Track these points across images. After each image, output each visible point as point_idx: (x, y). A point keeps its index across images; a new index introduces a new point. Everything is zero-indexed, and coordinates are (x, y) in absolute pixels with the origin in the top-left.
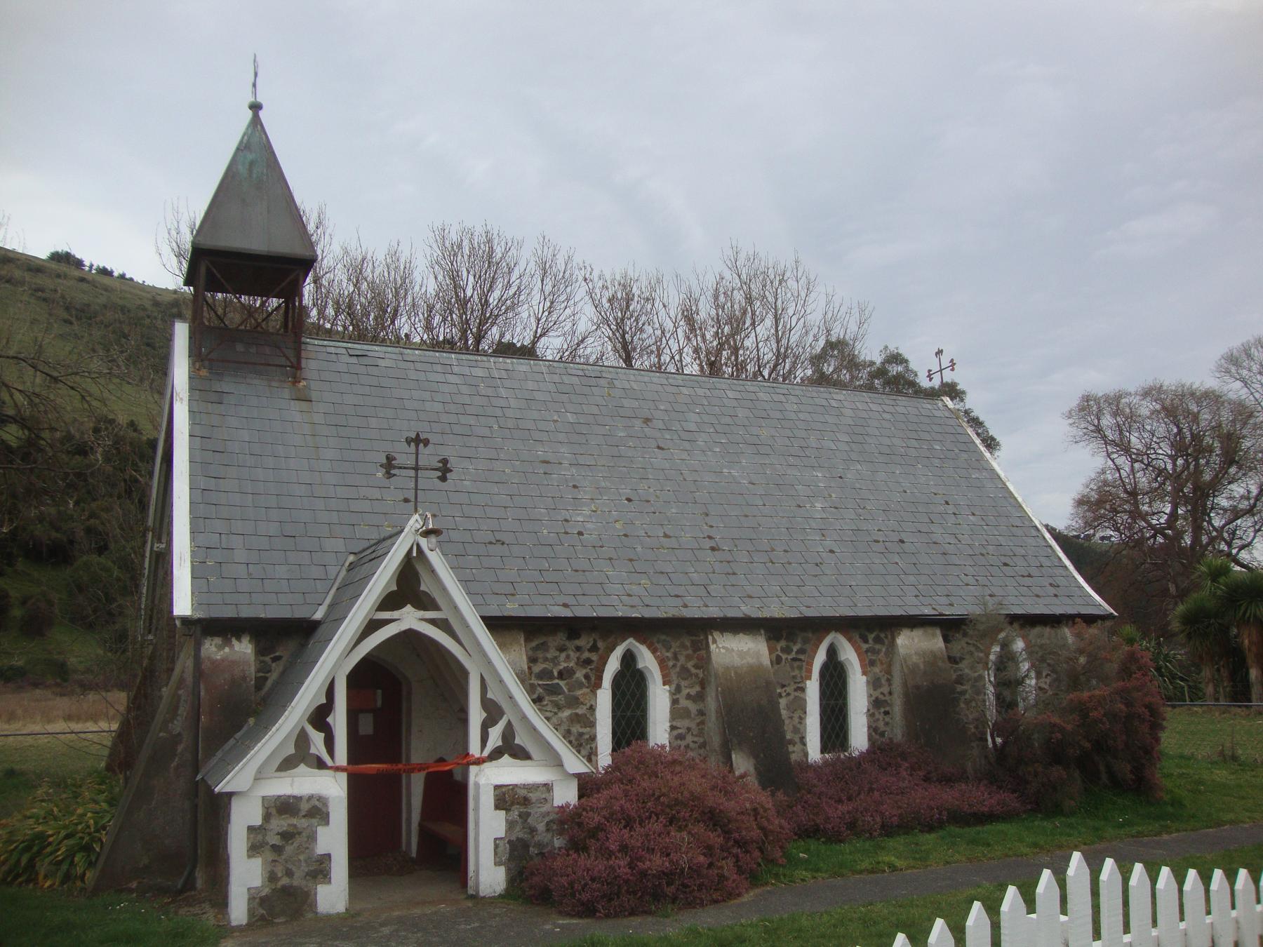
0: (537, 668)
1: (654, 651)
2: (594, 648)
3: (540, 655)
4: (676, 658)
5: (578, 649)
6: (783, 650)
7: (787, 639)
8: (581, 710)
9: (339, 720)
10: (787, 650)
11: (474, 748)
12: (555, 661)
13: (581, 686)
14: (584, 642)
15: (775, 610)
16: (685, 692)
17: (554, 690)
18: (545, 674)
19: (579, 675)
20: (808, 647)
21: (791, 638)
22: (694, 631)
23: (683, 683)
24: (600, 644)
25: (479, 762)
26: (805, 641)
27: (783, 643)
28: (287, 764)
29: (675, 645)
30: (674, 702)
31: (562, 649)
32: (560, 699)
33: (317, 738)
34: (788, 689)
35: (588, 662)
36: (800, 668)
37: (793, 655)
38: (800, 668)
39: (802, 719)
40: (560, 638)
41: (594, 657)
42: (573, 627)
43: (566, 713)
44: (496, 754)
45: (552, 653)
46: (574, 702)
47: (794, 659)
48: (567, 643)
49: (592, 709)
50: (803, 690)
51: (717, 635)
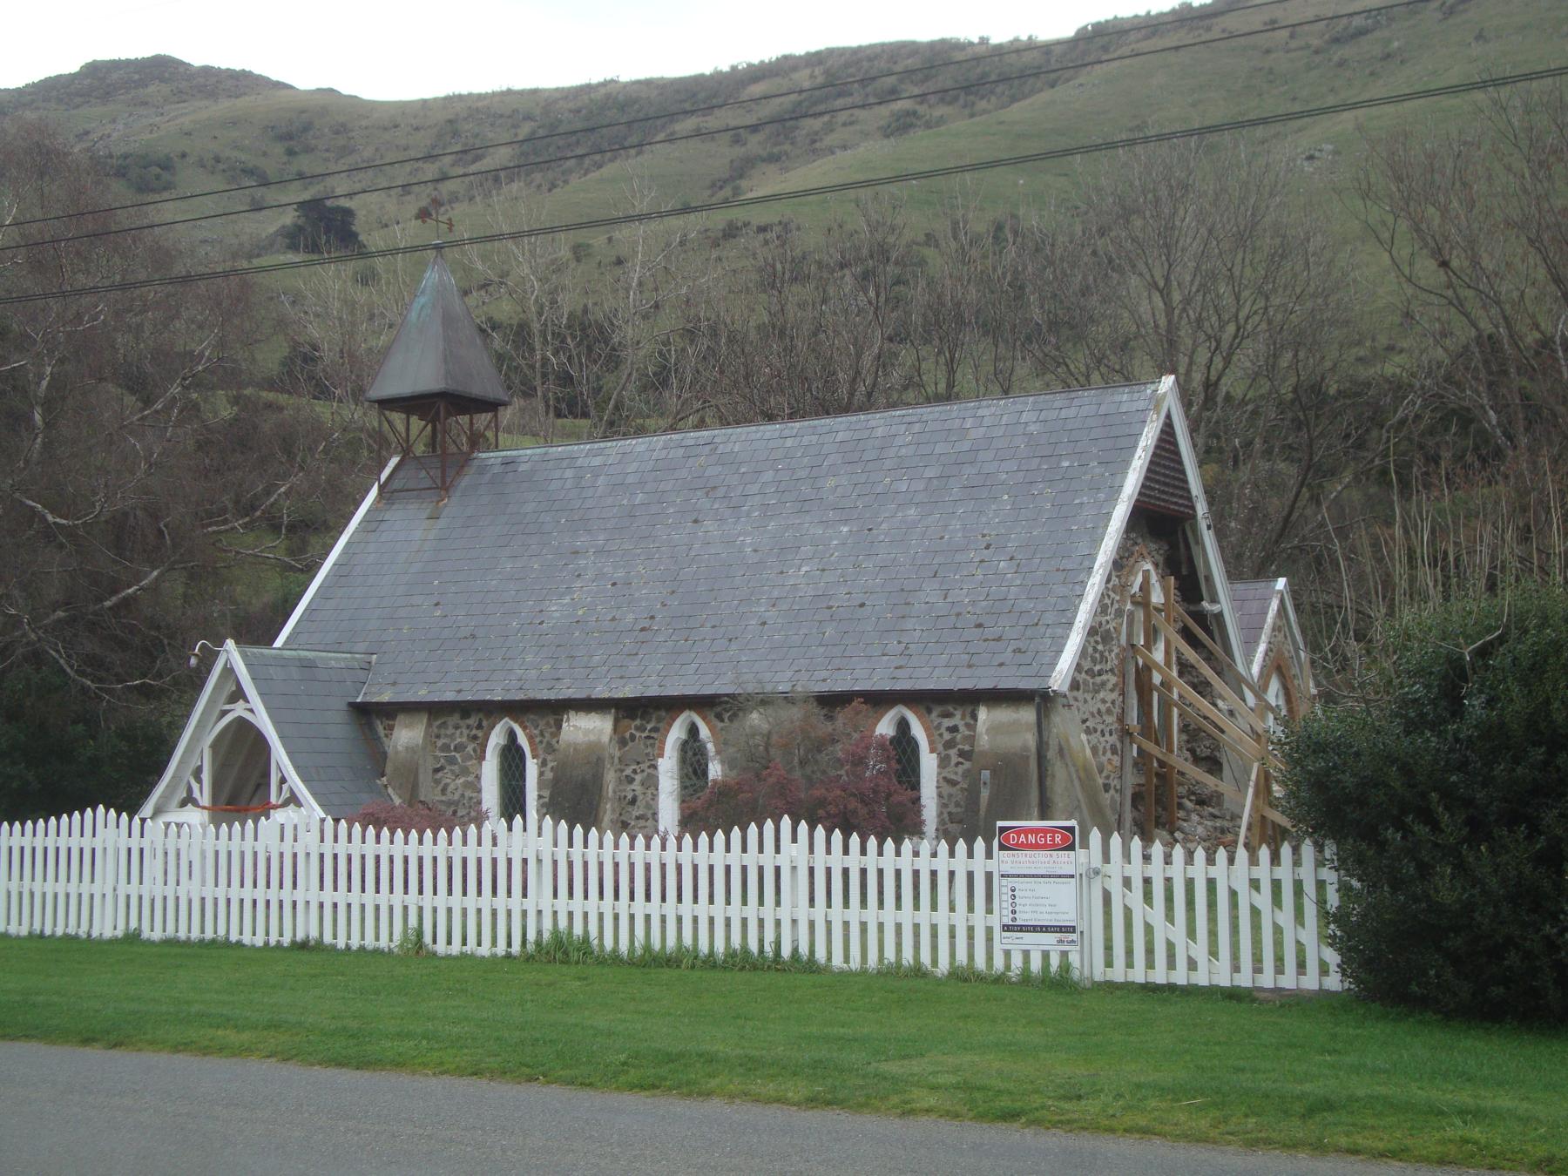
0: (440, 743)
1: (524, 728)
2: (480, 727)
3: (443, 731)
4: (542, 734)
5: (468, 727)
6: (637, 728)
7: (642, 718)
8: (471, 778)
9: (206, 776)
10: (641, 729)
11: (273, 800)
12: (452, 736)
13: (471, 758)
14: (472, 721)
15: (628, 691)
16: (550, 765)
17: (452, 761)
18: (446, 748)
19: (470, 749)
20: (661, 725)
21: (645, 716)
22: (559, 708)
23: (549, 758)
24: (485, 723)
25: (276, 807)
26: (659, 720)
27: (638, 722)
28: (183, 804)
29: (542, 723)
30: (541, 774)
31: (457, 728)
32: (456, 768)
33: (195, 786)
34: (643, 766)
35: (475, 738)
36: (653, 745)
37: (646, 734)
38: (653, 745)
39: (655, 797)
40: (455, 719)
41: (480, 733)
42: (465, 709)
43: (461, 781)
44: (285, 804)
45: (450, 731)
46: (465, 771)
47: (648, 737)
48: (462, 723)
49: (478, 777)
50: (655, 767)
51: (572, 714)
